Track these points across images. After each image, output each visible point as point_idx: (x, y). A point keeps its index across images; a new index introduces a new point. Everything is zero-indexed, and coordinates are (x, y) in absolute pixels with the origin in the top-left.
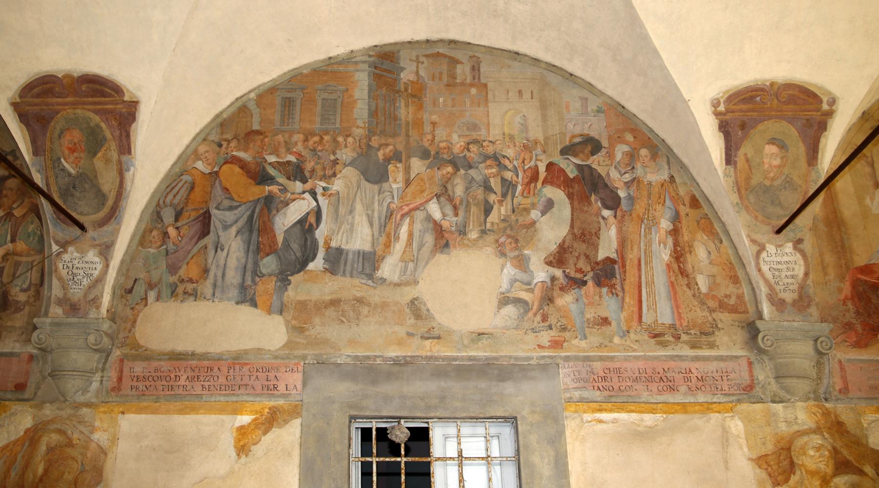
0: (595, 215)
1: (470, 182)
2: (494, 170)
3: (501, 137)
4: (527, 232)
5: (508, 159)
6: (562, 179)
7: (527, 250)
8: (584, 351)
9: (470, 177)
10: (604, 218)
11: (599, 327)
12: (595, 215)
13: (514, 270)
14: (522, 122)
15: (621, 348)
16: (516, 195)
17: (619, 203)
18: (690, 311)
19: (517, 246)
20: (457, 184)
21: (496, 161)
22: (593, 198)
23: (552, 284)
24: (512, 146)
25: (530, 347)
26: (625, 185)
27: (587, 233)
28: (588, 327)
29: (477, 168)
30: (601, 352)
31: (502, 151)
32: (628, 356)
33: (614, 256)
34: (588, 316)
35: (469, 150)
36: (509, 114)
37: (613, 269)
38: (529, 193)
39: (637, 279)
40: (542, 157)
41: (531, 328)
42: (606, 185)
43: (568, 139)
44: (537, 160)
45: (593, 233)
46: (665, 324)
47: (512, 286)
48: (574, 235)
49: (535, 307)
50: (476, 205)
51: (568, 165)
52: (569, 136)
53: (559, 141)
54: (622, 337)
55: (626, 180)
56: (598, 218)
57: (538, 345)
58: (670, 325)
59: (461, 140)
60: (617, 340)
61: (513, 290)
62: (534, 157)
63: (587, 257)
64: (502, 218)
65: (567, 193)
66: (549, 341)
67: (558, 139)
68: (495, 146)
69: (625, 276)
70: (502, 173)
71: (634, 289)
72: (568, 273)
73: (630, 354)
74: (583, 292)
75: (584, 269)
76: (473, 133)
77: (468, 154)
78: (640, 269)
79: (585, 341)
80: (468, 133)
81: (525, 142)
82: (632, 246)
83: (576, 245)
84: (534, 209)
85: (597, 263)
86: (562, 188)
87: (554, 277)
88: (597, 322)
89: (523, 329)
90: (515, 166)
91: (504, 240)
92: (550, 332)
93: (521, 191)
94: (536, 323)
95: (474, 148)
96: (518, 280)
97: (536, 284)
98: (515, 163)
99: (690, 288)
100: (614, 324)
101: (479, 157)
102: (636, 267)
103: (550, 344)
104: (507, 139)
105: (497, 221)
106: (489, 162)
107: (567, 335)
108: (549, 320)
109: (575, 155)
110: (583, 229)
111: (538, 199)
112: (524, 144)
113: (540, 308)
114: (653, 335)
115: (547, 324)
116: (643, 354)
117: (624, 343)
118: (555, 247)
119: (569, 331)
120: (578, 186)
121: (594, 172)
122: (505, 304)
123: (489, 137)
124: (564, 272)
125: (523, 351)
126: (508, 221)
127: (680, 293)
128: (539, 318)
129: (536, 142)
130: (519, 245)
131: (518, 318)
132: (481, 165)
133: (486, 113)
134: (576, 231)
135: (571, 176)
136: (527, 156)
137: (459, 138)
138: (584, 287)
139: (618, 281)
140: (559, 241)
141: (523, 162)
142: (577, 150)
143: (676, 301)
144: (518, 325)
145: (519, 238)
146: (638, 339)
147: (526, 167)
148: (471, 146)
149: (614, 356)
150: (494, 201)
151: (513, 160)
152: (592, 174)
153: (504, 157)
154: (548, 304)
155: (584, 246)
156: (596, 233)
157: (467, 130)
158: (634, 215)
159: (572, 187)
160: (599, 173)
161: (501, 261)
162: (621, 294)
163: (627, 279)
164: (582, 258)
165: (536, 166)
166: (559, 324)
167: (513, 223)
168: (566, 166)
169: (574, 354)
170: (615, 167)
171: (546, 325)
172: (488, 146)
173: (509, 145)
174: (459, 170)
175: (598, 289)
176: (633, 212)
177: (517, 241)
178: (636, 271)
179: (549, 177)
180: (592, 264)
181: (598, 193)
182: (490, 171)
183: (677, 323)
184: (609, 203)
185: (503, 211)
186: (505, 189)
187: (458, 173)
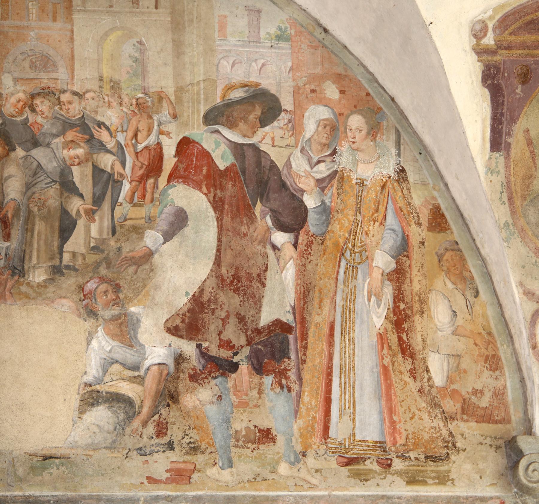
0: (260, 242)
1: (35, 174)
2: (80, 152)
3: (94, 85)
4: (136, 273)
5: (107, 128)
6: (204, 171)
7: (135, 305)
8: (227, 487)
9: (35, 164)
10: (275, 248)
11: (254, 446)
12: (260, 242)
13: (111, 341)
14: (137, 55)
15: (291, 483)
16: (120, 200)
17: (304, 220)
18: (412, 418)
19: (118, 297)
20: (10, 177)
21: (84, 133)
22: (259, 208)
23: (177, 369)
24: (114, 104)
25: (133, 481)
26: (316, 186)
27: (242, 274)
28: (237, 446)
29: (48, 145)
30: (256, 490)
31: (96, 112)
32: (302, 497)
33: (288, 318)
34: (238, 426)
35: (33, 109)
36: (113, 37)
37: (285, 343)
38: (144, 197)
39: (325, 361)
40: (171, 127)
41: (138, 446)
42: (284, 185)
43: (219, 92)
44: (161, 133)
45: (255, 276)
46: (367, 442)
47: (105, 372)
48: (221, 278)
49: (145, 410)
50: (45, 219)
51: (218, 145)
52: (223, 86)
53: (202, 96)
54: (292, 464)
55: (319, 176)
56: (265, 248)
57: (148, 478)
58: (376, 442)
59: (18, 88)
60: (283, 469)
61: (107, 379)
62: (156, 127)
63: (241, 319)
64: (92, 245)
65: (211, 199)
66: (167, 471)
67: (202, 92)
68: (83, 103)
69: (305, 354)
70: (95, 156)
71: (319, 378)
72: (206, 348)
73: (304, 493)
74: (230, 383)
75: (234, 342)
76: (43, 75)
77: (32, 118)
78: (331, 343)
79: (229, 470)
80: (32, 75)
81: (140, 95)
82: (321, 301)
83: (222, 297)
84: (149, 228)
85: (258, 332)
86: (204, 189)
87: (180, 355)
88: (252, 437)
89: (123, 448)
90: (119, 144)
91: (95, 286)
92: (169, 453)
93: (130, 193)
94: (145, 439)
95: (42, 105)
96: (117, 361)
97: (148, 369)
98: (121, 137)
99: (415, 378)
100: (281, 440)
101: (53, 124)
102: (325, 339)
103: (168, 475)
104: (106, 90)
105: (83, 250)
106: (71, 135)
107: (199, 459)
108: (169, 433)
109: (232, 125)
110: (237, 269)
111: (158, 210)
112: (137, 100)
113: (155, 411)
114: (346, 460)
115: (166, 439)
116: (326, 493)
117: (296, 474)
118: (185, 300)
119: (203, 453)
120: (233, 186)
121: (263, 160)
122: (93, 405)
123: (73, 84)
124: (199, 346)
125: (122, 487)
126: (103, 251)
127: (397, 386)
128: (151, 429)
129: (160, 97)
130: (121, 296)
131: (115, 429)
132: (57, 140)
133: (69, 34)
134: (224, 271)
135: (222, 165)
136: (143, 126)
137: (15, 84)
138: (234, 375)
139: (293, 364)
140: (193, 289)
141: (135, 136)
142: (235, 114)
143: (389, 399)
144: (114, 442)
145: (121, 284)
146: (319, 467)
147: (140, 147)
148: (37, 101)
149: (278, 496)
150: (78, 211)
151: (116, 131)
152: (259, 163)
153: (100, 124)
154: (168, 405)
155: (237, 300)
156: (259, 275)
157: (30, 67)
158: (328, 243)
159: (222, 189)
160: (272, 161)
161: (88, 324)
162: (295, 388)
163: (308, 360)
164: (233, 320)
165: (159, 145)
166: (186, 440)
167: (111, 254)
168: (213, 146)
169: (209, 493)
170: (303, 150)
171: (163, 442)
172: (70, 103)
173: (109, 102)
174: (14, 150)
175: (256, 379)
176: (328, 236)
177: (117, 288)
178: (325, 347)
179: (181, 167)
180: (249, 333)
181: (268, 200)
182: (72, 152)
183: (388, 440)
184: (286, 219)
185: (94, 233)
186: (99, 187)
187: (13, 155)
